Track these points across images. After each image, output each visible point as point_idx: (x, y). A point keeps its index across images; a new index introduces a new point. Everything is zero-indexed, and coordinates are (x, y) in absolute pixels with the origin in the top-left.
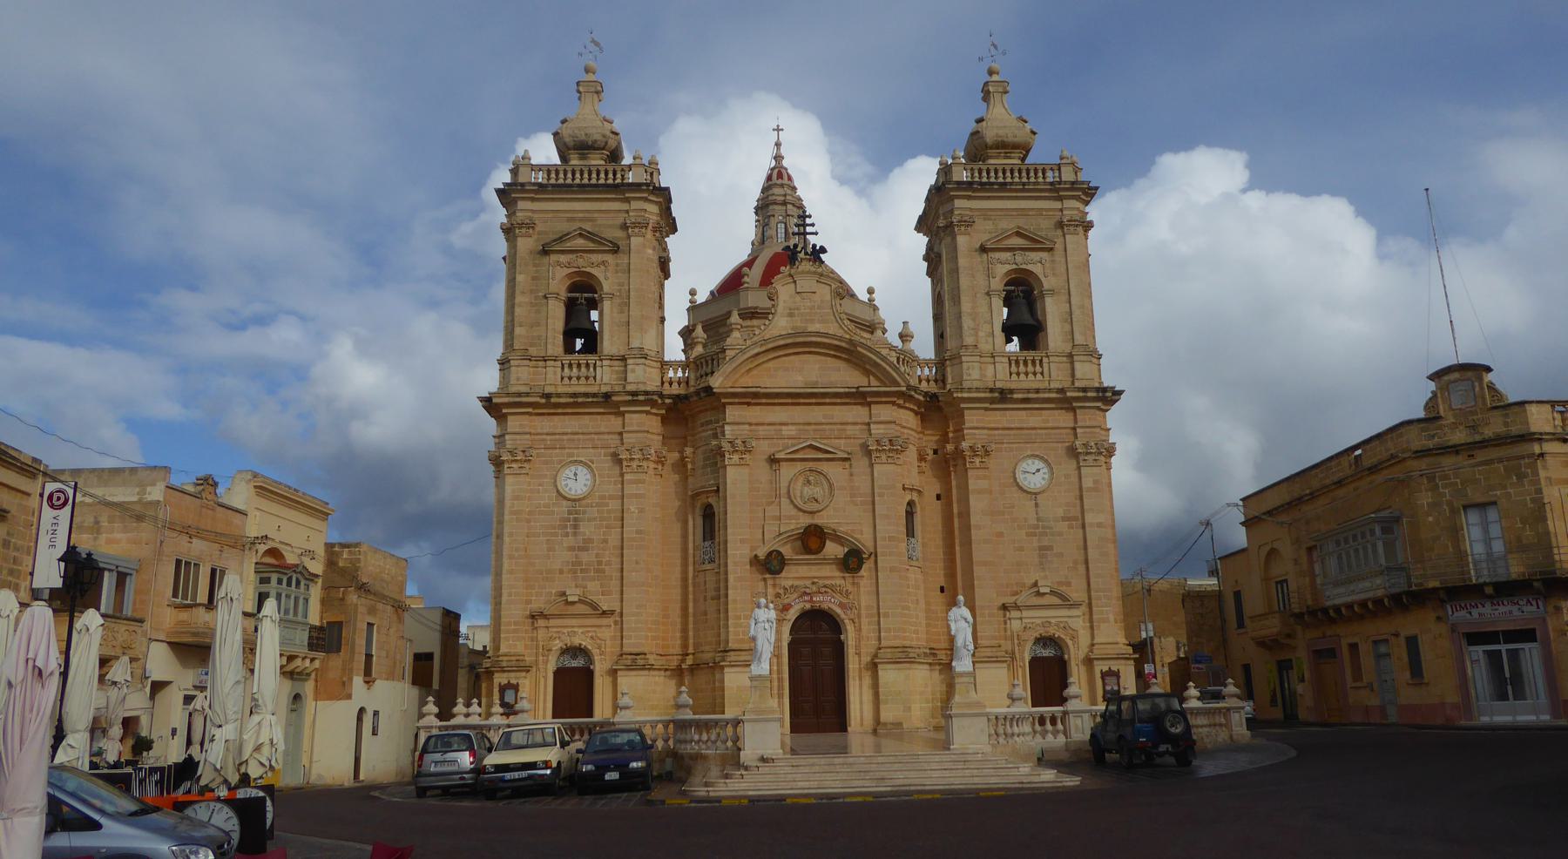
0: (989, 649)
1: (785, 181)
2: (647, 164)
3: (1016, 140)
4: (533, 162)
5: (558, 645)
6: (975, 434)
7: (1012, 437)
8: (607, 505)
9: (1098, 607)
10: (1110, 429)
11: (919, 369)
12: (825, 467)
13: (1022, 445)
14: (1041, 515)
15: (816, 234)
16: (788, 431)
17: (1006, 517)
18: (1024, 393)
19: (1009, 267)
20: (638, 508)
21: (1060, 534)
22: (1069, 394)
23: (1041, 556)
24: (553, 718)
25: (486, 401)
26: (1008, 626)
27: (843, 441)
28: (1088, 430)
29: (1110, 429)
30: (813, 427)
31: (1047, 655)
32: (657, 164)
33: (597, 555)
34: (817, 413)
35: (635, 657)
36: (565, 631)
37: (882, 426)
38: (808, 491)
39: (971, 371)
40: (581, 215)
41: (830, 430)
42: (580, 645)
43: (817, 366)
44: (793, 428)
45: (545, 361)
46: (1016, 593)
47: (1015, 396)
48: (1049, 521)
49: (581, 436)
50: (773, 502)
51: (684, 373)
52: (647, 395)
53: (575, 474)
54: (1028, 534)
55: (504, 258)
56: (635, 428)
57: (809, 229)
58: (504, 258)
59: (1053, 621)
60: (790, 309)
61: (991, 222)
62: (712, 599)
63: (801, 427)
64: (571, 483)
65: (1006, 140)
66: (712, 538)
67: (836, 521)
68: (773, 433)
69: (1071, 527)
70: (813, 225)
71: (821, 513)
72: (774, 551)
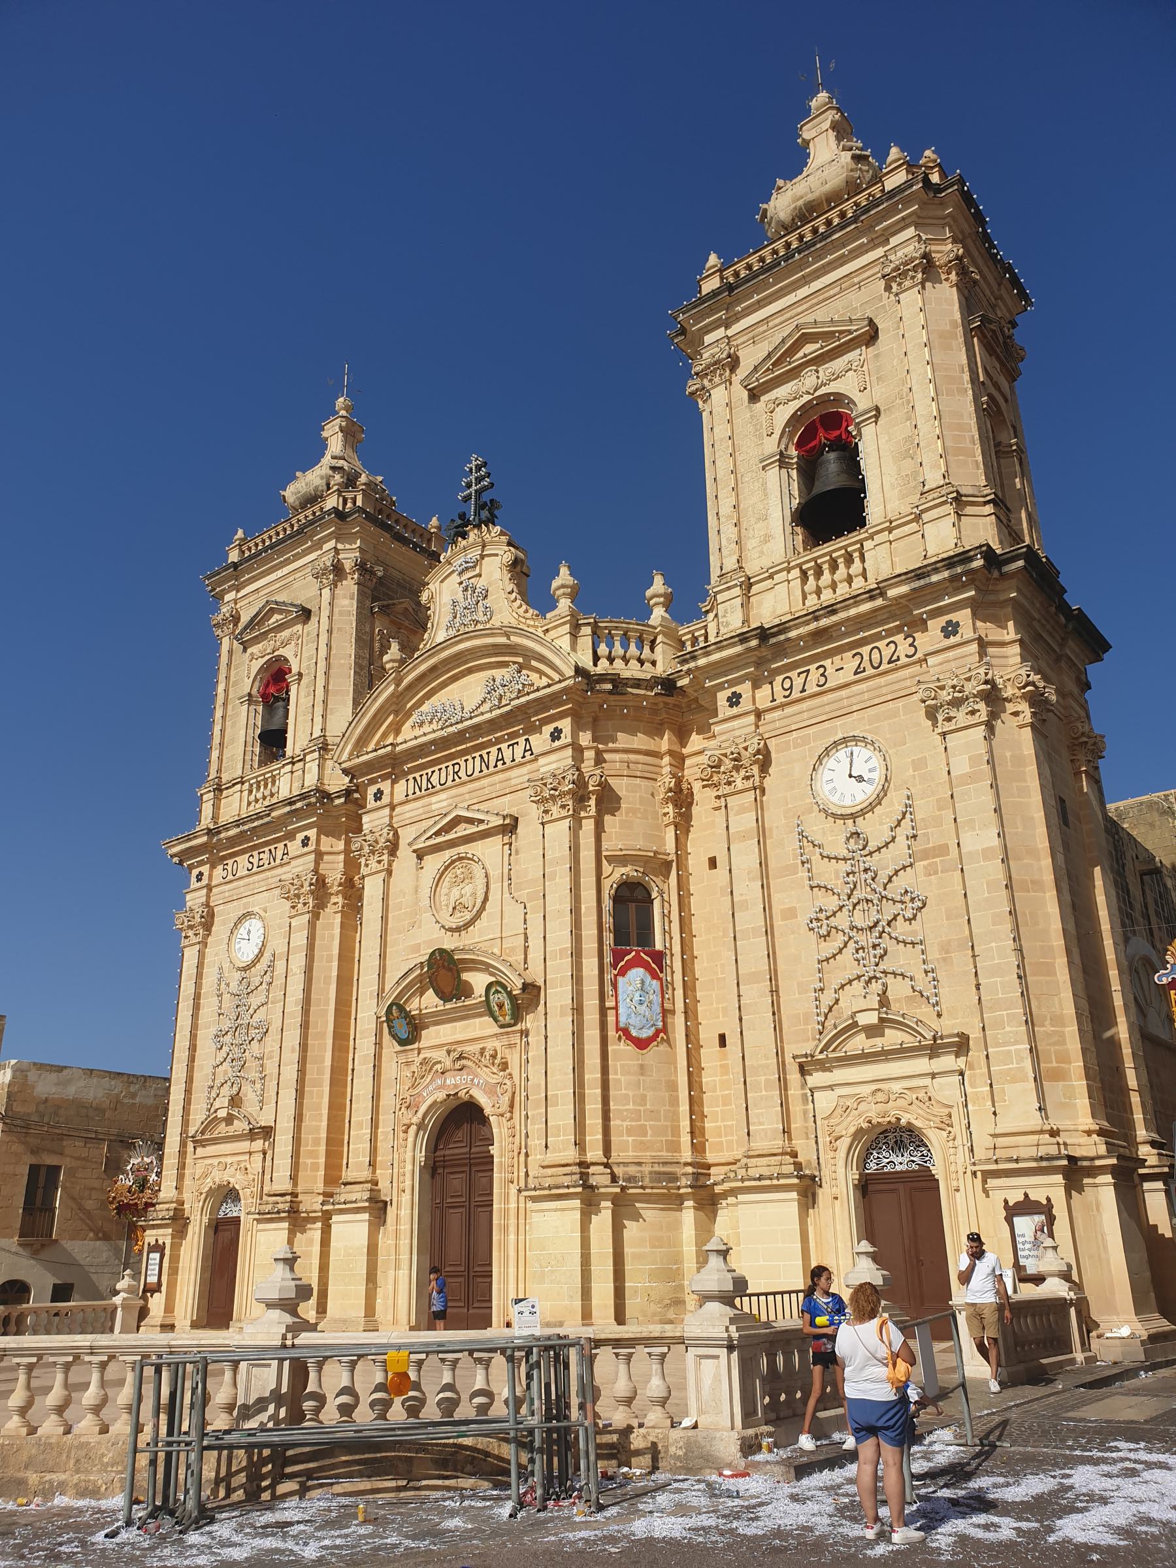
0: (765, 1161)
3: (827, 188)
5: (208, 1184)
9: (998, 1045)
12: (474, 849)
18: (807, 623)
19: (795, 405)
22: (892, 593)
36: (215, 1161)
38: (455, 893)
39: (729, 618)
40: (278, 585)
52: (304, 799)
65: (810, 197)
67: (491, 936)
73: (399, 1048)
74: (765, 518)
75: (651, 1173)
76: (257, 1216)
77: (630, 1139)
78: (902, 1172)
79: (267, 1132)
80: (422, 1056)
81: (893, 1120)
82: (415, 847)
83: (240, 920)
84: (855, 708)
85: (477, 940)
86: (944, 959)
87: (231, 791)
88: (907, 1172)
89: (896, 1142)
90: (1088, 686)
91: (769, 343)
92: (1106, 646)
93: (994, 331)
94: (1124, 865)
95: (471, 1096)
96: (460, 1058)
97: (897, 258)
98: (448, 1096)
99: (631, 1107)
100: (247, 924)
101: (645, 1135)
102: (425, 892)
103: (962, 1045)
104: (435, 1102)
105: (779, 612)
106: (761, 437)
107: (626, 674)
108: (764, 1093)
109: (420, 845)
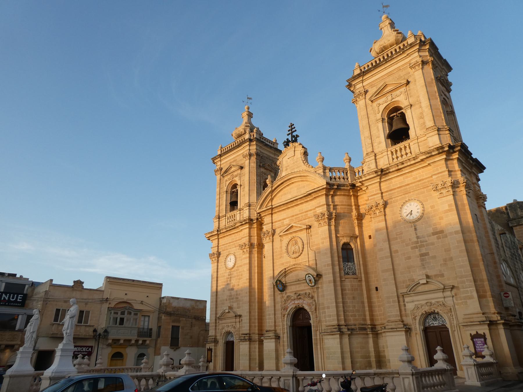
3: (390, 42)
5: (224, 331)
6: (374, 198)
7: (396, 194)
9: (464, 288)
13: (403, 196)
14: (419, 235)
16: (286, 222)
17: (398, 240)
21: (433, 244)
23: (422, 260)
26: (407, 307)
27: (307, 220)
28: (440, 175)
30: (295, 217)
31: (437, 325)
34: (296, 210)
35: (245, 335)
37: (321, 208)
40: (232, 160)
41: (302, 216)
42: (230, 331)
43: (296, 189)
44: (287, 220)
47: (391, 170)
48: (425, 237)
49: (231, 244)
54: (412, 248)
56: (246, 236)
57: (293, 130)
59: (433, 301)
60: (286, 167)
63: (290, 218)
65: (385, 45)
67: (305, 261)
68: (281, 224)
69: (438, 238)
70: (294, 128)
71: (299, 258)
73: (280, 292)
74: (379, 137)
75: (359, 328)
76: (240, 341)
77: (352, 318)
78: (436, 326)
79: (240, 316)
80: (287, 295)
81: (433, 311)
82: (280, 235)
83: (227, 256)
84: (411, 191)
85: (301, 262)
86: (445, 264)
87: (222, 219)
88: (438, 326)
89: (434, 317)
90: (479, 180)
91: (376, 87)
92: (484, 168)
93: (443, 79)
94: (495, 232)
95: (303, 306)
96: (299, 295)
97: (413, 61)
98: (296, 306)
99: (351, 309)
100: (230, 257)
101: (356, 317)
102: (284, 248)
103: (453, 287)
104: (292, 308)
105: (385, 164)
106: (376, 114)
107: (340, 183)
108: (392, 304)
109: (282, 234)
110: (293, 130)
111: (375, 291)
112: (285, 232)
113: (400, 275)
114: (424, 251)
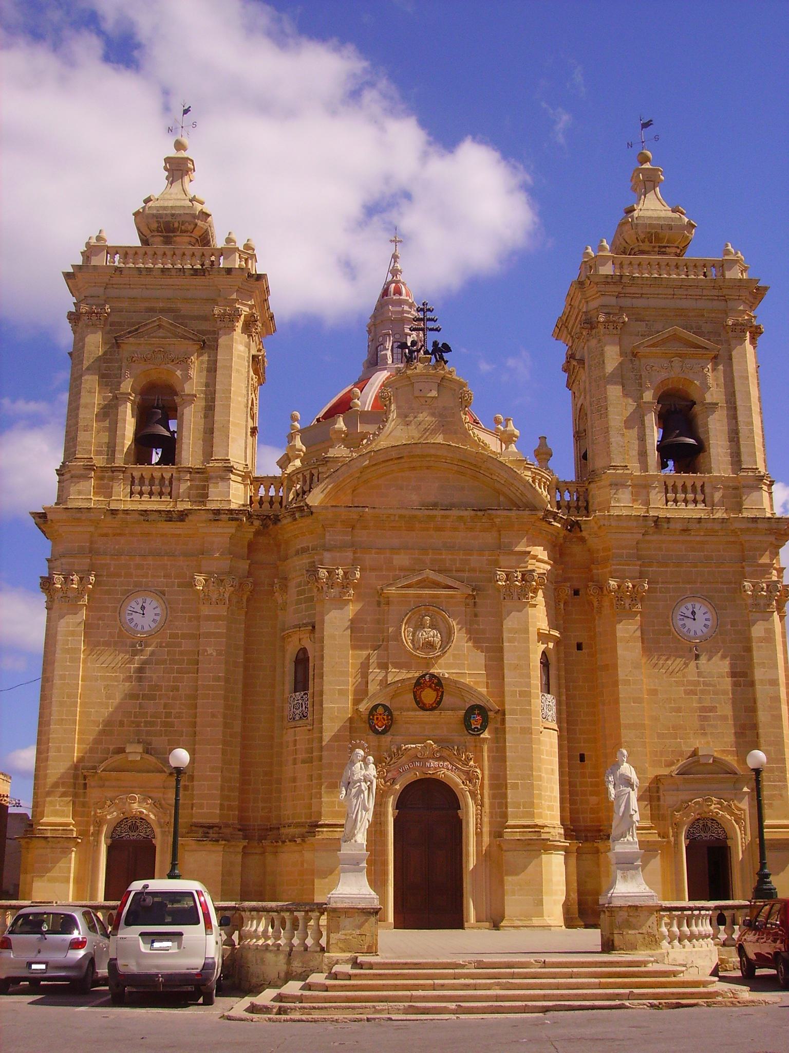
1: (404, 297)
2: (241, 248)
4: (109, 244)
8: (179, 645)
10: (785, 568)
11: (558, 494)
15: (438, 330)
20: (217, 650)
23: (703, 719)
24: (105, 900)
25: (40, 517)
26: (662, 802)
29: (785, 568)
32: (254, 250)
33: (166, 706)
45: (113, 472)
46: (671, 764)
50: (379, 646)
51: (277, 491)
53: (143, 608)
55: (70, 354)
58: (70, 354)
61: (644, 324)
62: (304, 762)
64: (137, 618)
66: (305, 688)
72: (379, 705)
83: (128, 594)
86: (742, 733)
89: (704, 825)
110: (431, 325)
111: (579, 762)
112: (401, 587)
113: (656, 740)
114: (707, 704)
